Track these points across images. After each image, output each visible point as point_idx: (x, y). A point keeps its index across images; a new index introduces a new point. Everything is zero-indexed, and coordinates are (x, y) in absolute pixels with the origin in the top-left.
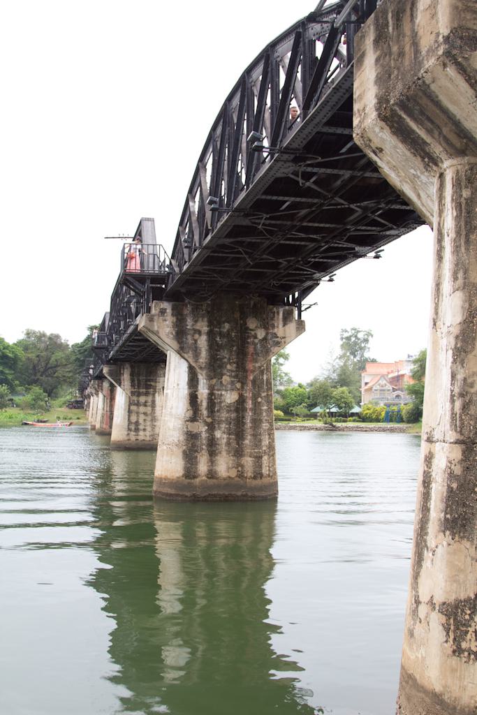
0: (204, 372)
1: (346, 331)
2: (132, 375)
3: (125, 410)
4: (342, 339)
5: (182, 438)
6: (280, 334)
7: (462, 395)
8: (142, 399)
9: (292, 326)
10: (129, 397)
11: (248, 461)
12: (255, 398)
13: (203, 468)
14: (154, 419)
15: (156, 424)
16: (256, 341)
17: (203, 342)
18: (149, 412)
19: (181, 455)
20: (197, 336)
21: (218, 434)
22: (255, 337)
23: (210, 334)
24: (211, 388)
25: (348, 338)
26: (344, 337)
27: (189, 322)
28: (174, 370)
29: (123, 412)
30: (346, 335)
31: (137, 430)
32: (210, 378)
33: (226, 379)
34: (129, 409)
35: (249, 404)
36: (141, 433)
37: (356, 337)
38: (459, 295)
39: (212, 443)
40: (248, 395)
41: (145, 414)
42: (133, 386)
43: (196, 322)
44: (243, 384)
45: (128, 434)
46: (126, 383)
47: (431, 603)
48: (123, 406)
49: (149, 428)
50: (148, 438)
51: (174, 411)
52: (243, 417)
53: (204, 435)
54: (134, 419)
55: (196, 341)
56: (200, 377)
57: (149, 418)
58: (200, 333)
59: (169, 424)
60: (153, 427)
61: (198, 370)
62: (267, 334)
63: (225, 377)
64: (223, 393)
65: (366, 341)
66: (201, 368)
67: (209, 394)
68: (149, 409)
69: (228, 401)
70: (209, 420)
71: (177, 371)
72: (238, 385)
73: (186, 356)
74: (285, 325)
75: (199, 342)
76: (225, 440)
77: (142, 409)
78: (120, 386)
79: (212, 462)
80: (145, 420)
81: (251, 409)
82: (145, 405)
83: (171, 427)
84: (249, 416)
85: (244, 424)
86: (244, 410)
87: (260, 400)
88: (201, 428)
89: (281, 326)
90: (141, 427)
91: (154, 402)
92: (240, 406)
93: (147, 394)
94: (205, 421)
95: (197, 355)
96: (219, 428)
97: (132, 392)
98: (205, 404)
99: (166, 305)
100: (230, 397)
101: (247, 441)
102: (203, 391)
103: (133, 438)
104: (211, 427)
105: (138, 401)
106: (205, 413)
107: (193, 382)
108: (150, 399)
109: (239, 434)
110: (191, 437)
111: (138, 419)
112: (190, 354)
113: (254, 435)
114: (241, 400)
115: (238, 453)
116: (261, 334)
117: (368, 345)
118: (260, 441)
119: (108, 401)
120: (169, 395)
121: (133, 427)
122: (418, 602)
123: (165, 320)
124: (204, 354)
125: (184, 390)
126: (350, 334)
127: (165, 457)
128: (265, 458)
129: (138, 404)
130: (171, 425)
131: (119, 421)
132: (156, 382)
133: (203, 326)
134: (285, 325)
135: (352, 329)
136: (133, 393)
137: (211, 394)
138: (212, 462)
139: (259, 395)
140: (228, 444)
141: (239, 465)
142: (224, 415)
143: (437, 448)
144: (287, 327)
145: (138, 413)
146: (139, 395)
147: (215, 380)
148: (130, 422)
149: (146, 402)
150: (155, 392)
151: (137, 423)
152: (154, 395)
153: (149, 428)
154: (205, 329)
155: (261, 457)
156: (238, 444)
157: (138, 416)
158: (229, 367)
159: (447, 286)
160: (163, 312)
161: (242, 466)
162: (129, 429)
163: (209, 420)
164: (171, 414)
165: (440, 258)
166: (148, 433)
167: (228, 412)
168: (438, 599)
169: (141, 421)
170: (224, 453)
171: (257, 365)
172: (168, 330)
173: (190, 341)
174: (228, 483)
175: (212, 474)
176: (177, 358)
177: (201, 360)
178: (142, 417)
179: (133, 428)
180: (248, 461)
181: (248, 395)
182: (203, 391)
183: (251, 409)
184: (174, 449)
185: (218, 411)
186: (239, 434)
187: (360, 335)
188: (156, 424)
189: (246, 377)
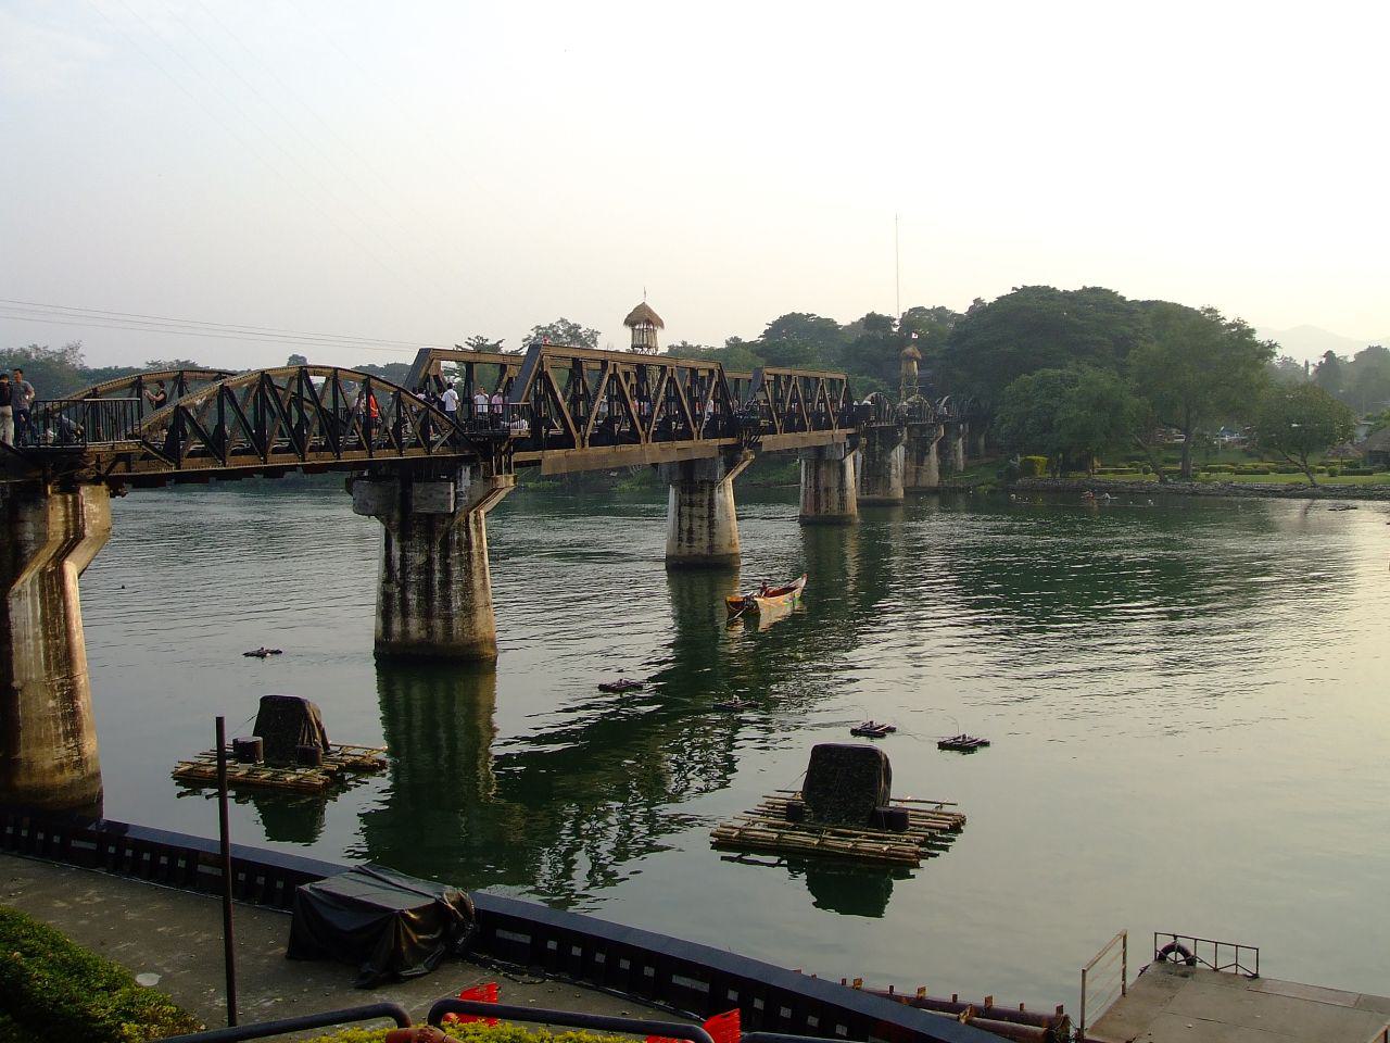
8: (696, 497)
11: (438, 623)
12: (445, 556)
13: (397, 627)
14: (712, 525)
21: (410, 596)
24: (403, 549)
31: (690, 540)
32: (402, 539)
35: (437, 567)
39: (404, 602)
40: (436, 556)
41: (701, 518)
45: (679, 545)
49: (705, 537)
52: (432, 579)
54: (686, 525)
57: (706, 523)
60: (711, 535)
68: (706, 509)
72: (426, 547)
76: (415, 602)
77: (696, 511)
79: (405, 624)
84: (438, 576)
85: (432, 586)
86: (432, 571)
87: (448, 561)
93: (702, 491)
100: (418, 559)
102: (396, 553)
103: (685, 551)
104: (404, 590)
106: (398, 574)
109: (426, 592)
110: (386, 597)
115: (427, 614)
118: (450, 602)
121: (685, 536)
129: (691, 505)
137: (403, 558)
138: (405, 624)
139: (448, 556)
140: (419, 605)
141: (429, 628)
142: (413, 577)
151: (690, 531)
152: (712, 490)
156: (427, 605)
161: (431, 627)
162: (680, 539)
166: (705, 544)
167: (420, 573)
174: (421, 643)
175: (405, 633)
178: (697, 523)
180: (438, 623)
181: (436, 556)
185: (409, 573)
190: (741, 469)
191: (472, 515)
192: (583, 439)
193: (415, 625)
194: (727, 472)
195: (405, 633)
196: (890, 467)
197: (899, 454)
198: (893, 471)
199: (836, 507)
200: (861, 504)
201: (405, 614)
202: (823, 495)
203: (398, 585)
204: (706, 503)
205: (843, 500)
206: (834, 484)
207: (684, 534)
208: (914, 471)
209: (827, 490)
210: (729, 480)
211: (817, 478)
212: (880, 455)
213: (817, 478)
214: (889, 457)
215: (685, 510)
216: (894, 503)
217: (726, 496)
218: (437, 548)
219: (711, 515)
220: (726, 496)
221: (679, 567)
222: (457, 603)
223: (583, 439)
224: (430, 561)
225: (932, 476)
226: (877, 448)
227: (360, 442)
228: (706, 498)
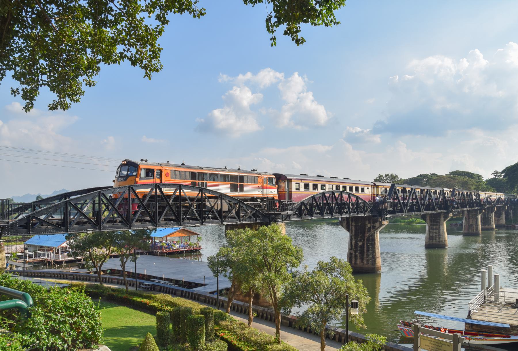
2: (430, 217)
8: (435, 227)
11: (365, 262)
13: (353, 262)
17: (353, 228)
21: (357, 254)
23: (356, 226)
24: (356, 241)
27: (350, 223)
31: (433, 239)
32: (355, 238)
33: (359, 238)
35: (365, 246)
36: (434, 241)
39: (356, 256)
42: (431, 221)
43: (352, 222)
44: (364, 240)
49: (438, 239)
50: (437, 243)
54: (431, 235)
55: (352, 228)
57: (438, 235)
60: (439, 238)
67: (355, 243)
68: (438, 231)
77: (434, 231)
80: (435, 235)
82: (436, 229)
85: (364, 251)
86: (364, 247)
88: (353, 252)
90: (434, 238)
91: (440, 228)
93: (436, 225)
98: (354, 245)
100: (360, 244)
101: (365, 256)
102: (354, 242)
104: (355, 252)
106: (353, 247)
107: (351, 240)
108: (438, 227)
113: (367, 255)
114: (363, 244)
115: (362, 259)
124: (354, 232)
129: (433, 229)
133: (353, 224)
136: (431, 225)
140: (360, 256)
142: (359, 248)
146: (433, 225)
148: (430, 236)
150: (440, 224)
151: (433, 237)
152: (440, 226)
153: (438, 239)
154: (354, 225)
157: (433, 234)
162: (429, 239)
169: (434, 236)
170: (359, 259)
172: (345, 225)
175: (355, 263)
186: (362, 253)
189: (365, 238)
190: (448, 219)
191: (375, 232)
192: (406, 211)
193: (359, 261)
194: (444, 220)
195: (355, 263)
196: (490, 218)
197: (493, 214)
198: (492, 220)
200: (482, 229)
203: (354, 251)
205: (477, 228)
207: (430, 238)
208: (497, 219)
209: (472, 225)
210: (445, 223)
211: (469, 222)
213: (469, 222)
216: (492, 229)
217: (444, 226)
218: (366, 240)
219: (439, 232)
220: (444, 226)
221: (428, 246)
222: (371, 256)
223: (406, 211)
224: (363, 244)
225: (503, 221)
227: (347, 211)
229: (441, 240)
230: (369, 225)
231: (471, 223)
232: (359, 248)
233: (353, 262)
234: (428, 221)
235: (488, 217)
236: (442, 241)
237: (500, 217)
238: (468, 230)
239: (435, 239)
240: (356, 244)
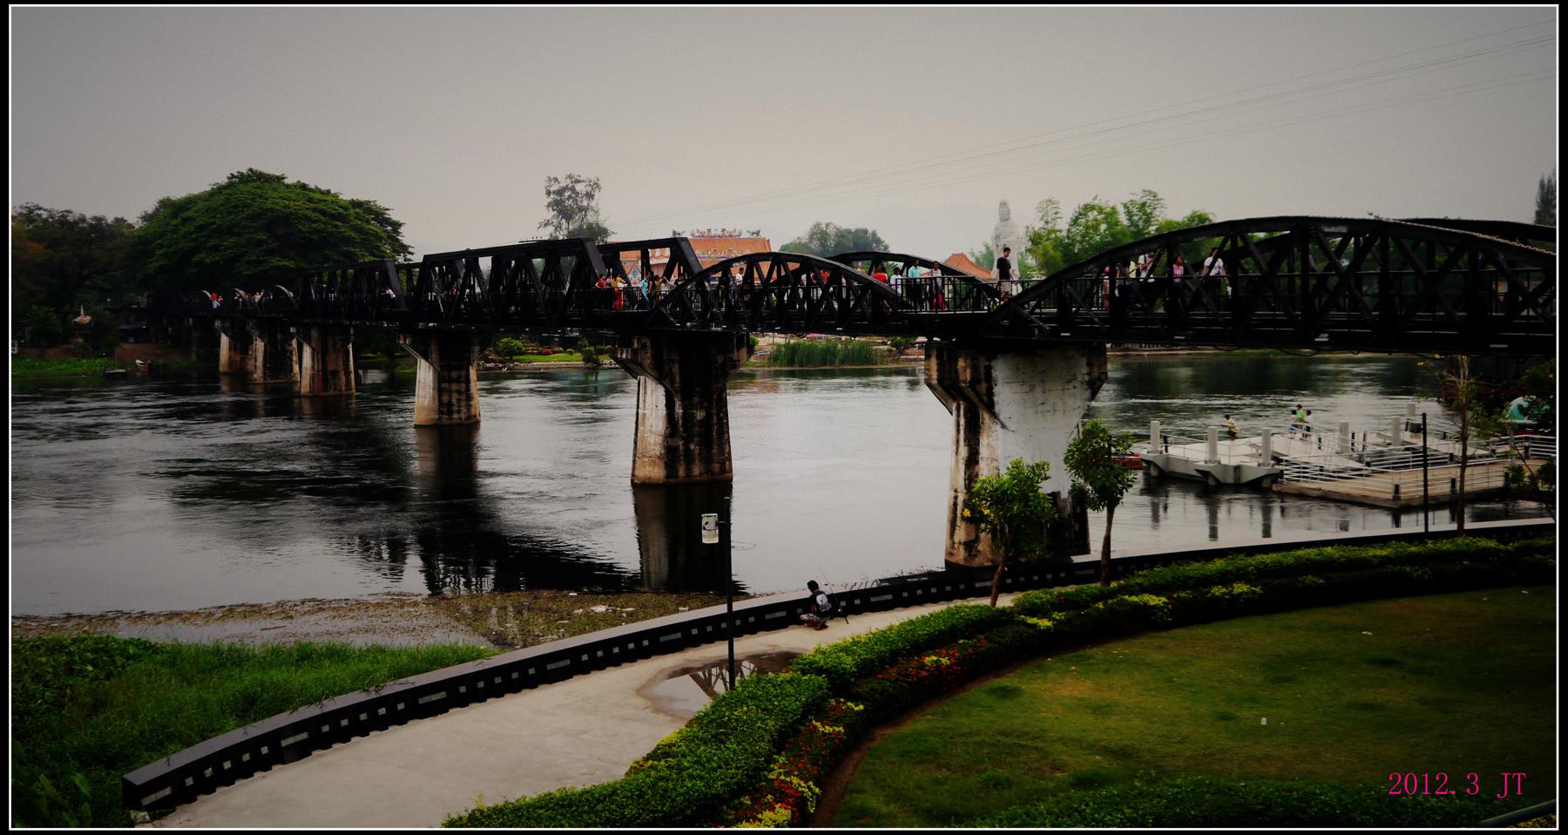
0: (679, 396)
1: (556, 180)
3: (434, 389)
4: (549, 193)
5: (663, 451)
6: (735, 358)
7: (968, 479)
8: (454, 374)
9: (744, 351)
10: (439, 373)
12: (718, 415)
13: (682, 473)
15: (471, 403)
16: (717, 365)
17: (676, 369)
18: (463, 390)
19: (663, 465)
20: (671, 365)
22: (716, 362)
25: (560, 192)
26: (552, 189)
28: (652, 394)
29: (431, 391)
30: (555, 187)
31: (450, 413)
32: (683, 400)
33: (696, 399)
34: (439, 386)
36: (455, 416)
37: (573, 189)
38: (966, 448)
39: (688, 453)
41: (459, 392)
42: (442, 358)
45: (440, 419)
46: (434, 356)
47: (960, 543)
48: (431, 384)
49: (464, 410)
51: (653, 429)
53: (681, 448)
54: (445, 399)
55: (671, 369)
56: (676, 399)
57: (464, 397)
58: (674, 362)
59: (649, 439)
60: (469, 407)
61: (674, 394)
62: (725, 358)
63: (695, 398)
64: (695, 412)
65: (590, 196)
66: (676, 392)
67: (684, 414)
68: (464, 385)
69: (699, 418)
70: (684, 435)
71: (654, 395)
72: (706, 405)
73: (664, 382)
74: (738, 351)
75: (674, 370)
76: (697, 451)
77: (454, 387)
78: (426, 359)
79: (688, 470)
80: (458, 400)
81: (716, 424)
82: (458, 381)
83: (652, 442)
89: (735, 352)
90: (455, 408)
91: (468, 376)
92: (707, 422)
94: (681, 436)
95: (673, 383)
96: (693, 441)
97: (441, 366)
99: (645, 340)
100: (700, 415)
102: (679, 411)
104: (686, 445)
105: (449, 376)
107: (670, 405)
108: (463, 373)
111: (450, 399)
112: (668, 380)
114: (708, 417)
115: (707, 460)
116: (720, 359)
117: (593, 204)
119: (320, 356)
120: (648, 415)
122: (954, 543)
123: (647, 353)
125: (662, 411)
126: (563, 184)
127: (647, 468)
128: (727, 463)
129: (450, 381)
130: (652, 442)
131: (426, 402)
132: (470, 352)
134: (738, 351)
135: (570, 177)
138: (688, 470)
140: (700, 453)
141: (709, 471)
143: (959, 494)
144: (740, 351)
145: (450, 392)
147: (687, 402)
149: (459, 377)
151: (450, 404)
153: (464, 410)
155: (725, 463)
157: (450, 396)
158: (698, 389)
159: (962, 442)
160: (644, 346)
162: (441, 412)
163: (684, 435)
164: (651, 431)
165: (958, 431)
166: (463, 416)
168: (963, 540)
169: (454, 401)
171: (719, 385)
173: (667, 370)
176: (654, 385)
177: (676, 385)
179: (445, 410)
182: (679, 411)
183: (716, 424)
184: (657, 461)
187: (580, 188)
188: (471, 403)
193: (697, 470)
196: (291, 353)
199: (343, 388)
201: (689, 463)
202: (329, 377)
203: (683, 438)
204: (463, 379)
206: (341, 367)
208: (238, 358)
209: (335, 373)
212: (281, 347)
213: (324, 363)
214: (291, 345)
215: (445, 385)
226: (279, 337)
228: (463, 373)
229: (473, 410)
230: (720, 359)
231: (331, 367)
232: (696, 429)
233: (682, 473)
234: (434, 356)
235: (285, 351)
236: (475, 416)
237: (247, 353)
238: (325, 387)
239: (459, 412)
240: (687, 416)
